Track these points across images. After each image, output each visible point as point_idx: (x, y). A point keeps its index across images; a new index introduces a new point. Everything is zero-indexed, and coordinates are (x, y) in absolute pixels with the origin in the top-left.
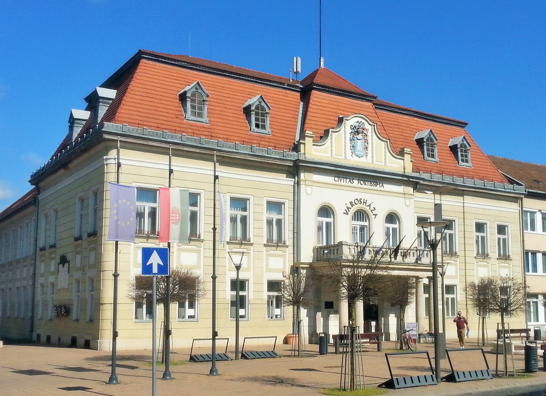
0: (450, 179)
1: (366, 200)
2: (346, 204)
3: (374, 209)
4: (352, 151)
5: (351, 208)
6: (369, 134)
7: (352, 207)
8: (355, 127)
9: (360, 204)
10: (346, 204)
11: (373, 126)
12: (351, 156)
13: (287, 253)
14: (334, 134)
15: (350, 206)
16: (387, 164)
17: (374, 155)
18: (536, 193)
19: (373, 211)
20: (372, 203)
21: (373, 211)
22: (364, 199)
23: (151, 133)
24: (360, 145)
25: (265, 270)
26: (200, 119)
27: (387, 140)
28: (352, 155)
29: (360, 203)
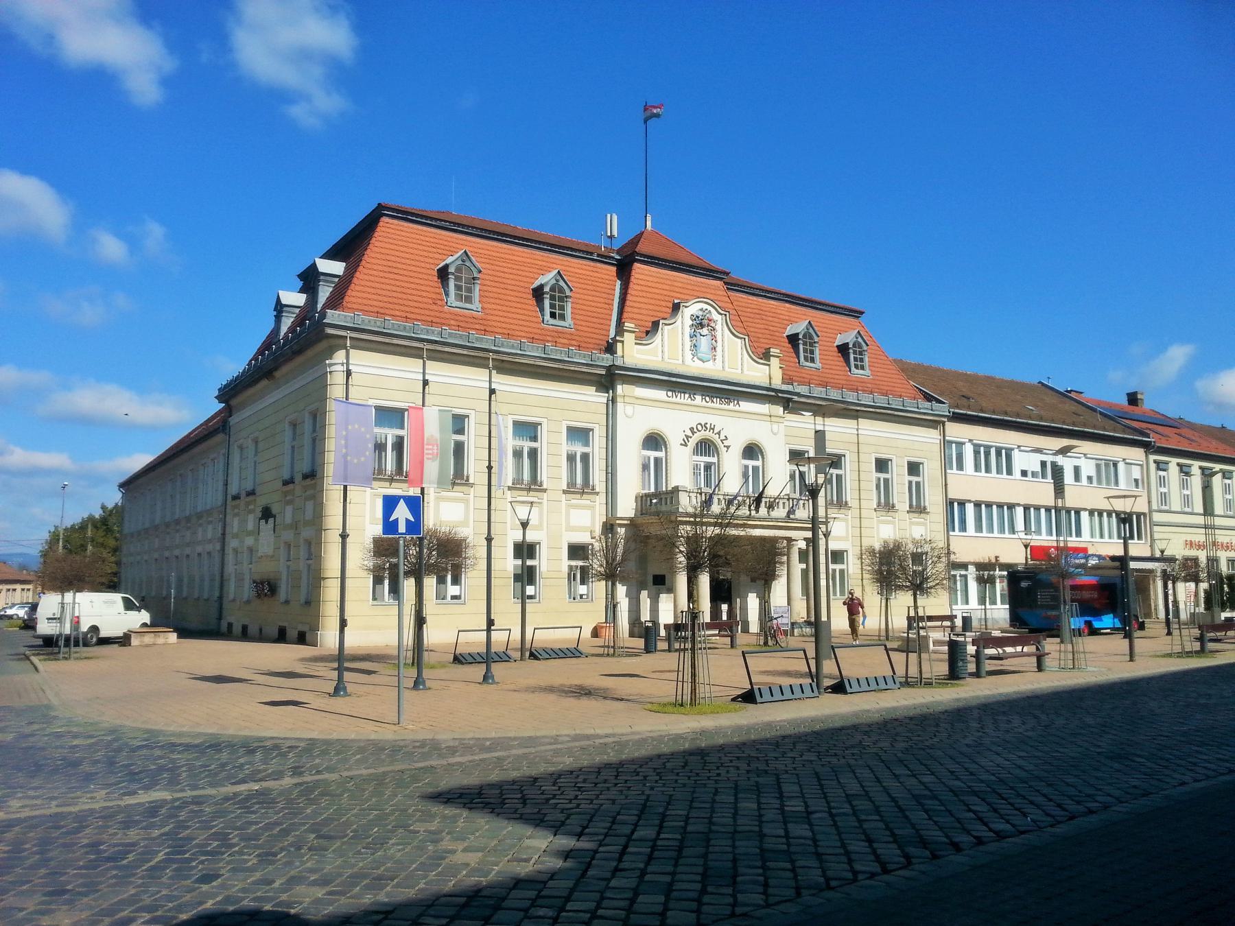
6: (718, 327)
8: (698, 317)
13: (597, 503)
14: (666, 328)
16: (746, 372)
17: (726, 359)
18: (966, 415)
23: (395, 326)
24: (704, 343)
25: (564, 529)
26: (468, 306)
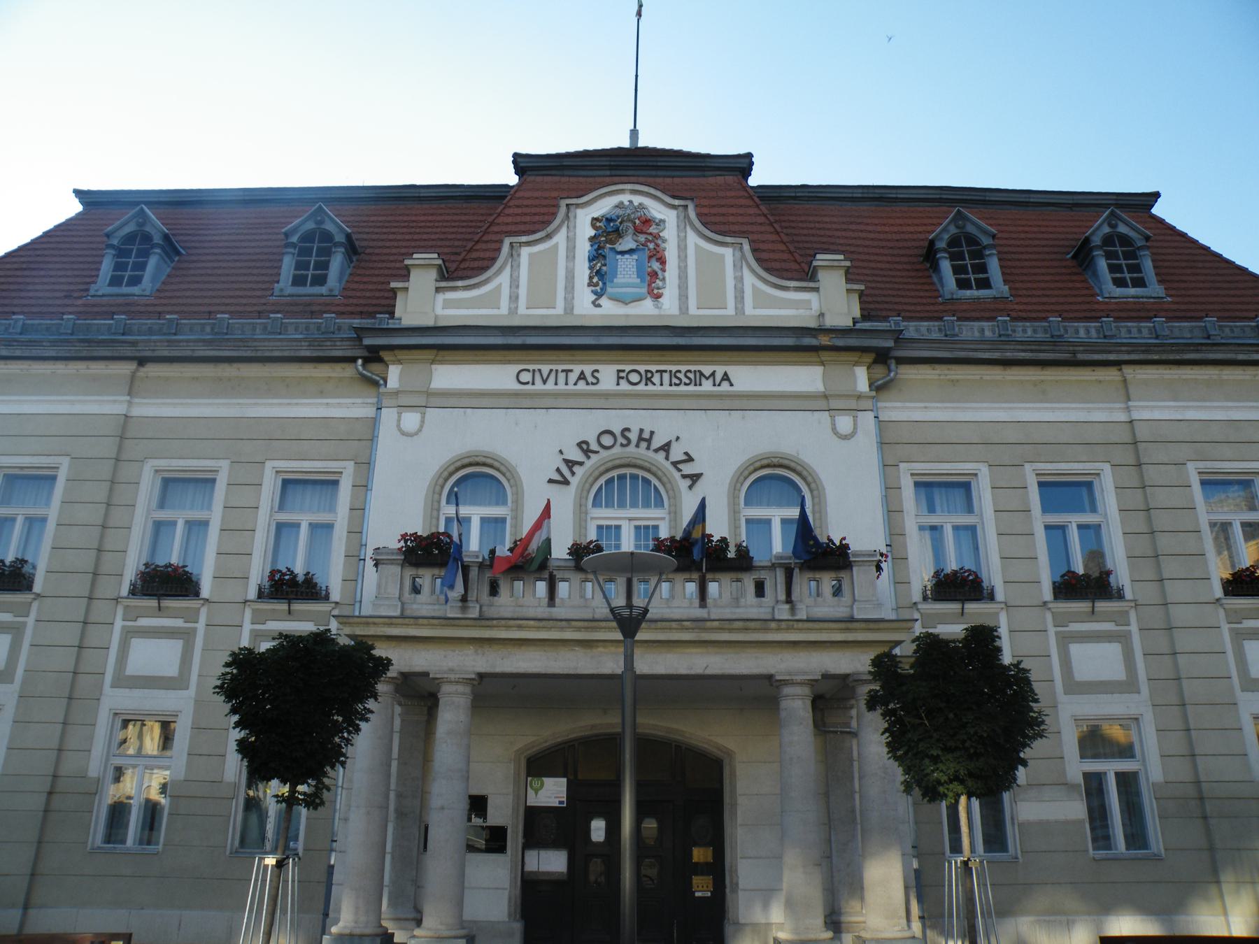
1: (652, 433)
3: (685, 457)
4: (598, 288)
5: (581, 464)
6: (670, 233)
9: (622, 445)
10: (561, 452)
11: (681, 209)
12: (593, 303)
15: (576, 455)
16: (749, 310)
19: (680, 466)
20: (678, 438)
21: (680, 466)
22: (641, 431)
28: (596, 299)
29: (625, 442)
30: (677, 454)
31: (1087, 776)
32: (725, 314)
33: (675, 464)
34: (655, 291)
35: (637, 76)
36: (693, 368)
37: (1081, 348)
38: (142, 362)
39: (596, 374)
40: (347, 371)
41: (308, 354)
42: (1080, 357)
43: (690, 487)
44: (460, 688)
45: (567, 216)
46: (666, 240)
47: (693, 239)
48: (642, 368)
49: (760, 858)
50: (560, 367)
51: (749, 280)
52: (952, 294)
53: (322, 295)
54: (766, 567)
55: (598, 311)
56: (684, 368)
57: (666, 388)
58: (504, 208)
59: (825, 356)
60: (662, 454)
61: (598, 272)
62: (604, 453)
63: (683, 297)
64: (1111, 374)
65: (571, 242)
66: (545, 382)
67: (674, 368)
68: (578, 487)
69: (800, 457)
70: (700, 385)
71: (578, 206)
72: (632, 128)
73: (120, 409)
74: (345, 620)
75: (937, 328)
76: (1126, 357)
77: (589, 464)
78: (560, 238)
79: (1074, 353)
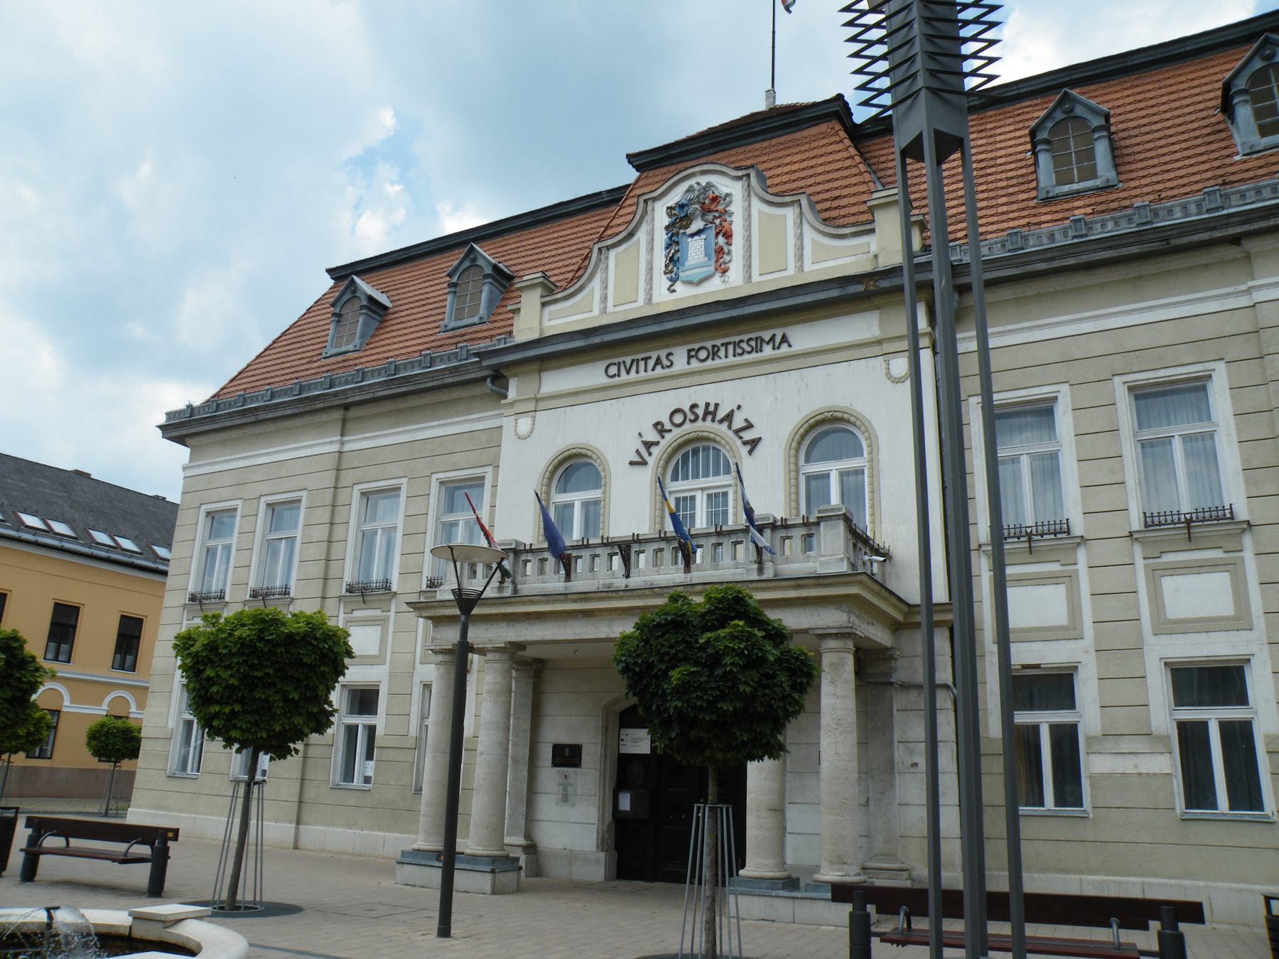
0: (1116, 224)
1: (717, 405)
2: (640, 434)
3: (744, 424)
5: (657, 443)
6: (737, 208)
7: (663, 437)
10: (640, 434)
19: (741, 434)
20: (739, 407)
22: (707, 405)
27: (796, 198)
28: (671, 286)
29: (692, 418)
30: (738, 422)
31: (1183, 727)
32: (789, 276)
33: (737, 432)
34: (723, 266)
35: (774, 32)
36: (753, 335)
37: (1175, 232)
38: (346, 407)
39: (671, 358)
40: (477, 390)
41: (450, 380)
42: (1174, 242)
43: (750, 452)
44: (497, 656)
45: (645, 212)
46: (732, 213)
47: (757, 205)
48: (709, 345)
49: (807, 803)
50: (640, 356)
51: (809, 234)
52: (1048, 192)
53: (475, 324)
54: (741, 530)
55: (674, 296)
56: (745, 337)
57: (732, 360)
58: (619, 210)
59: (878, 301)
60: (725, 425)
61: (671, 260)
62: (677, 432)
63: (748, 267)
64: (1230, 252)
65: (651, 234)
66: (628, 372)
67: (737, 339)
68: (654, 466)
69: (854, 407)
70: (761, 351)
71: (655, 199)
72: (770, 87)
73: (336, 447)
74: (414, 606)
75: (999, 245)
76: (1238, 230)
77: (664, 443)
78: (642, 235)
79: (1167, 240)
